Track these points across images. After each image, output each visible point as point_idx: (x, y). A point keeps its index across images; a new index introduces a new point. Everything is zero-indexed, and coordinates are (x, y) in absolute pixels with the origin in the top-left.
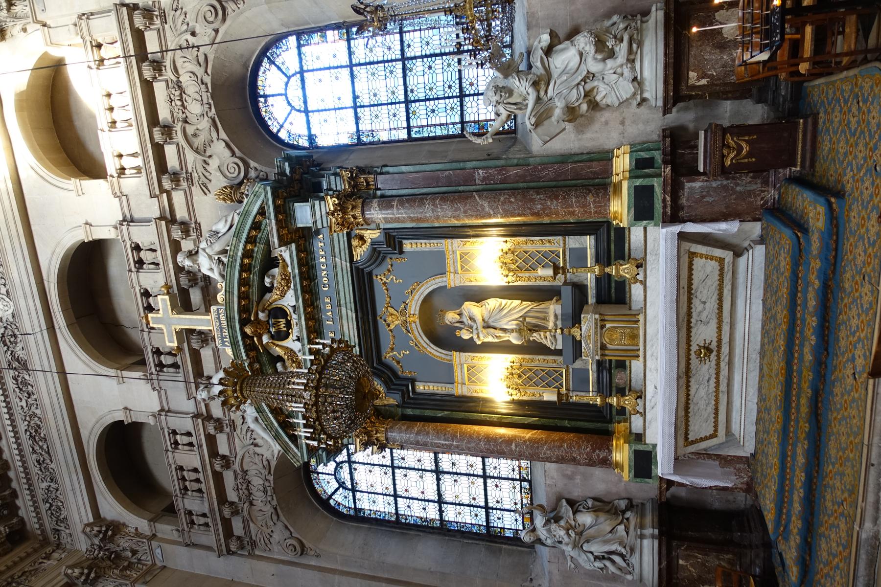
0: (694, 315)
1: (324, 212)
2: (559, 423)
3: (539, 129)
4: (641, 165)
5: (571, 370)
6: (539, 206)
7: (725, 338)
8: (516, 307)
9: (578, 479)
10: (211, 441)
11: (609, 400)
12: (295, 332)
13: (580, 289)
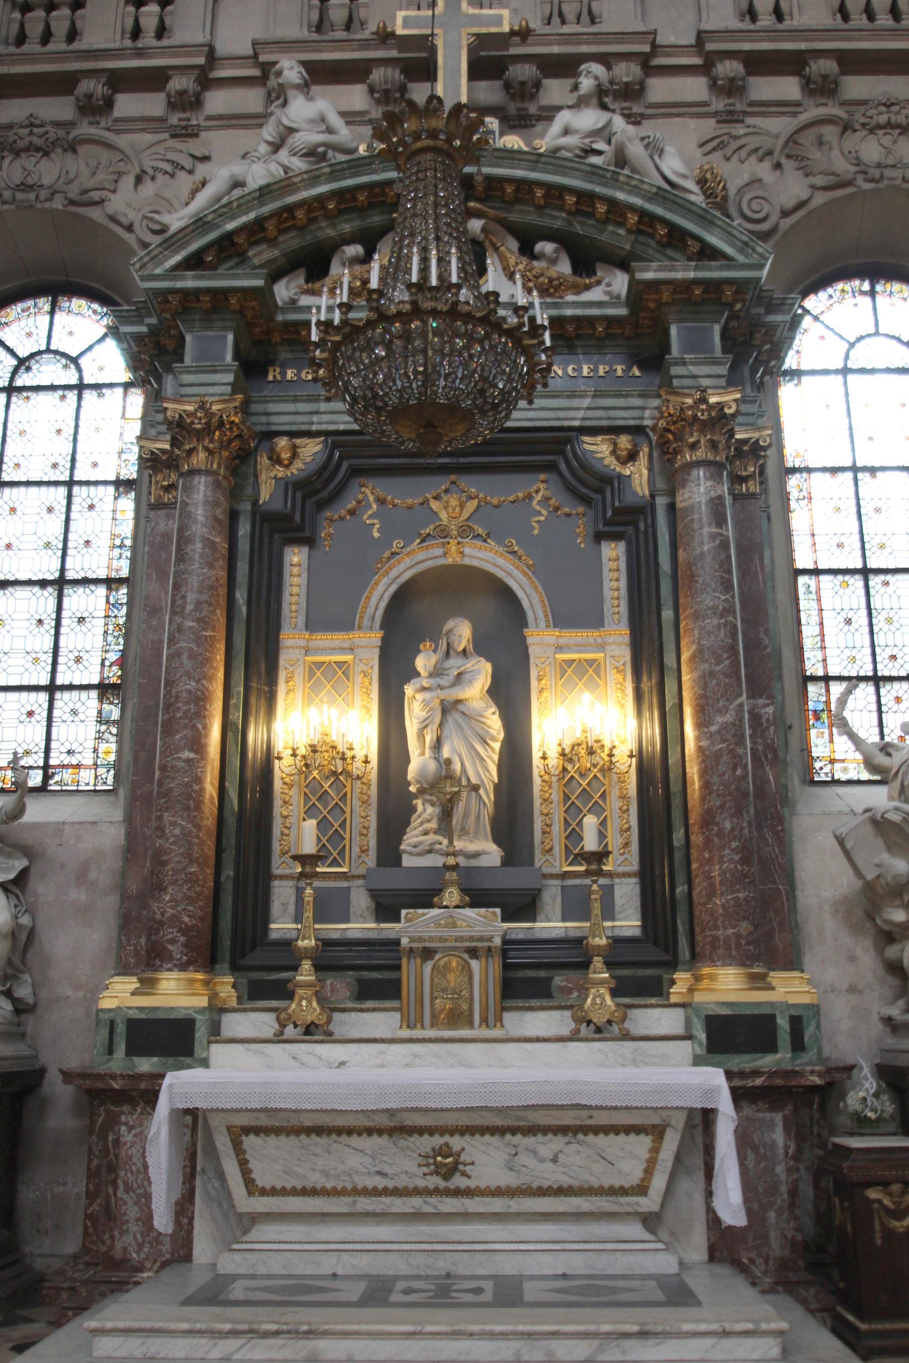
0: (530, 1141)
1: (705, 382)
2: (229, 856)
3: (869, 829)
5: (345, 884)
6: (728, 825)
7: (473, 1205)
8: (484, 767)
9: (80, 895)
10: (152, 80)
11: (307, 965)
13: (522, 906)
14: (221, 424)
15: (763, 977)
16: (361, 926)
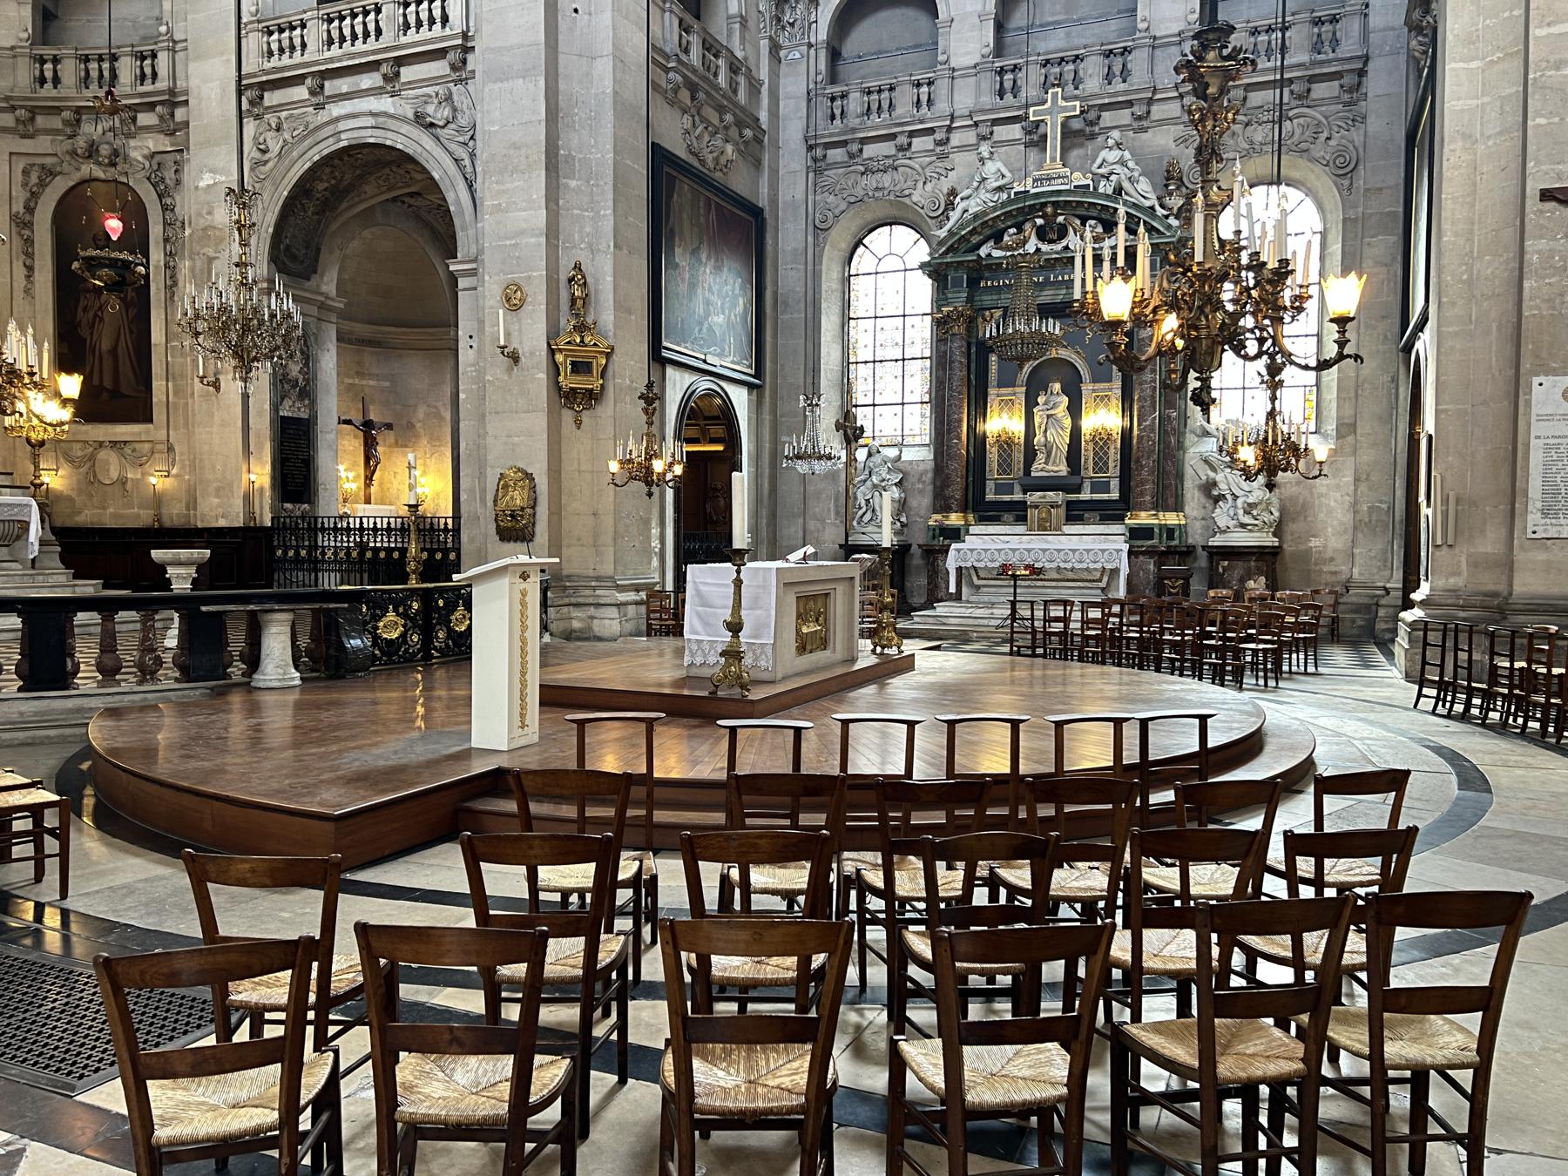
4: (1170, 531)
8: (1062, 440)
12: (1045, 247)
13: (1078, 490)
16: (1018, 496)
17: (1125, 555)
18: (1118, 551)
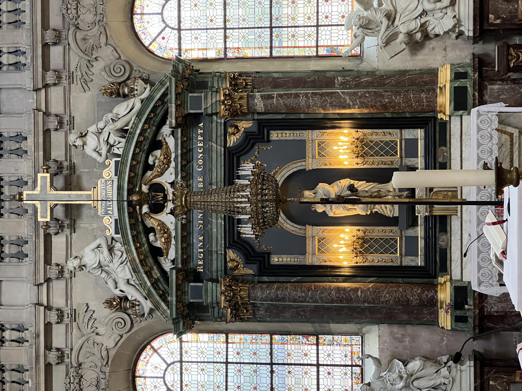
3: (387, 47)
4: (458, 76)
5: (404, 238)
6: (387, 100)
12: (170, 206)
14: (230, 286)
15: (441, 88)
16: (420, 231)
17: (483, 108)
18: (479, 115)
